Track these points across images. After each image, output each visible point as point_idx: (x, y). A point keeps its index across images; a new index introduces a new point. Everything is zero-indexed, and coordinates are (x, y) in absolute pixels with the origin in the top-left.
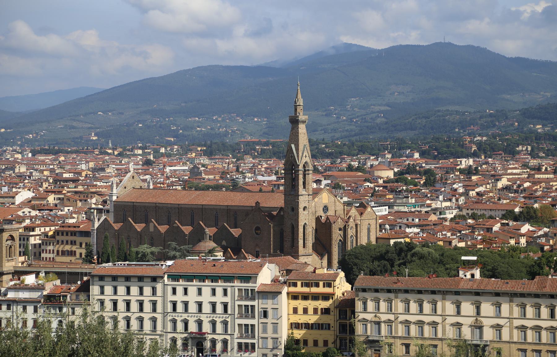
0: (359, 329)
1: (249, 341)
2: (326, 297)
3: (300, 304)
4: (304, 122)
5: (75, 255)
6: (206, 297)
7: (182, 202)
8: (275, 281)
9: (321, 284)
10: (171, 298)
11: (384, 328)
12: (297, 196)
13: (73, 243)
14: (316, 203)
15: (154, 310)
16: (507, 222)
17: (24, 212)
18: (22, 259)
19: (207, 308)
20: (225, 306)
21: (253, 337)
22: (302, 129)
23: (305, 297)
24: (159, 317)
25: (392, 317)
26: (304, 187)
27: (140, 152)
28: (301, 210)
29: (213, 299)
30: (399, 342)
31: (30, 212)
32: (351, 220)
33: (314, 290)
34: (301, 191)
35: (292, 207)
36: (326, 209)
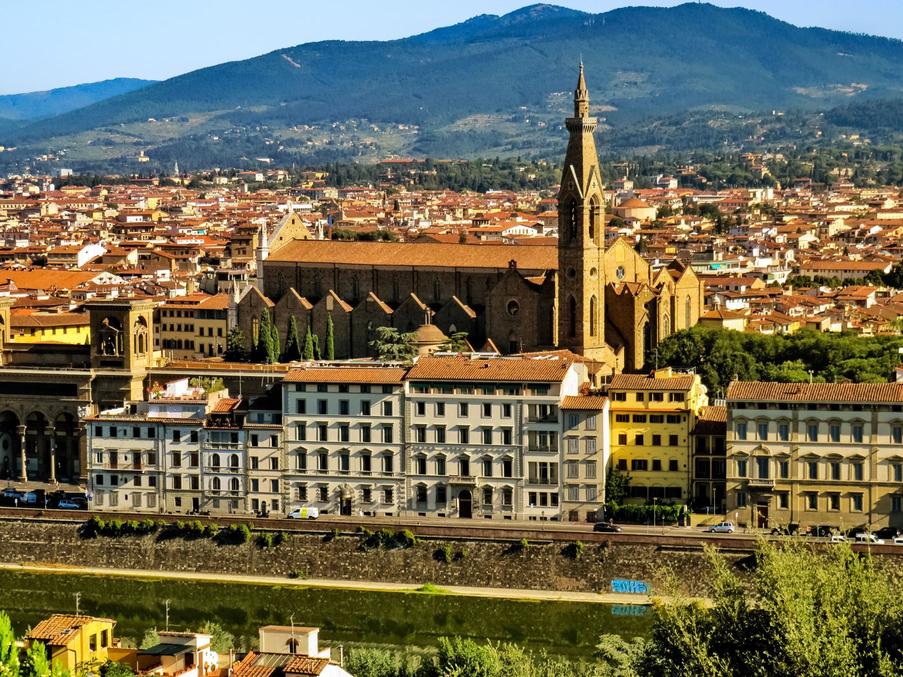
0: (732, 470)
1: (549, 491)
2: (673, 418)
3: (632, 431)
4: (590, 128)
5: (193, 348)
6: (475, 419)
7: (379, 262)
8: (586, 392)
9: (666, 396)
10: (414, 419)
11: (774, 468)
12: (580, 248)
13: (190, 328)
14: (607, 263)
15: (389, 439)
16: (885, 290)
17: (101, 279)
18: (157, 354)
19: (476, 438)
20: (507, 432)
21: (555, 483)
22: (588, 140)
23: (639, 419)
24: (396, 450)
25: (787, 450)
26: (592, 236)
27: (224, 180)
28: (586, 273)
29: (486, 422)
30: (799, 489)
31: (110, 279)
32: (665, 289)
33: (654, 406)
34: (587, 242)
35: (572, 268)
36: (621, 270)
